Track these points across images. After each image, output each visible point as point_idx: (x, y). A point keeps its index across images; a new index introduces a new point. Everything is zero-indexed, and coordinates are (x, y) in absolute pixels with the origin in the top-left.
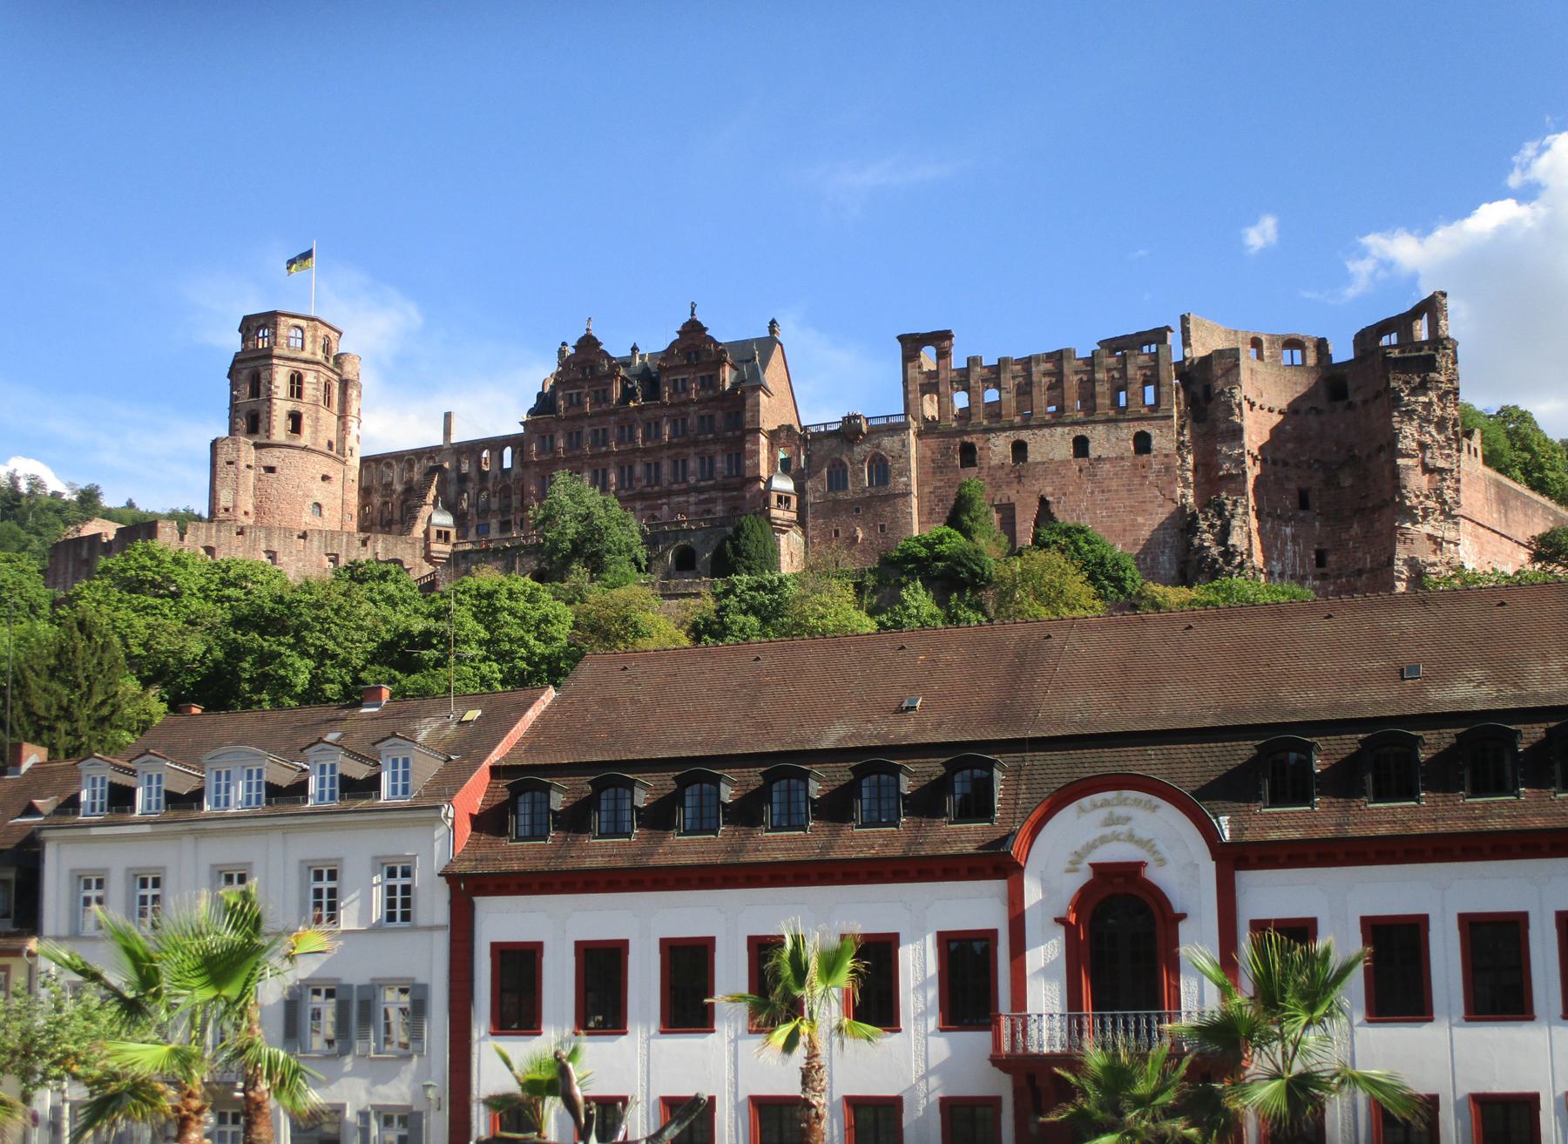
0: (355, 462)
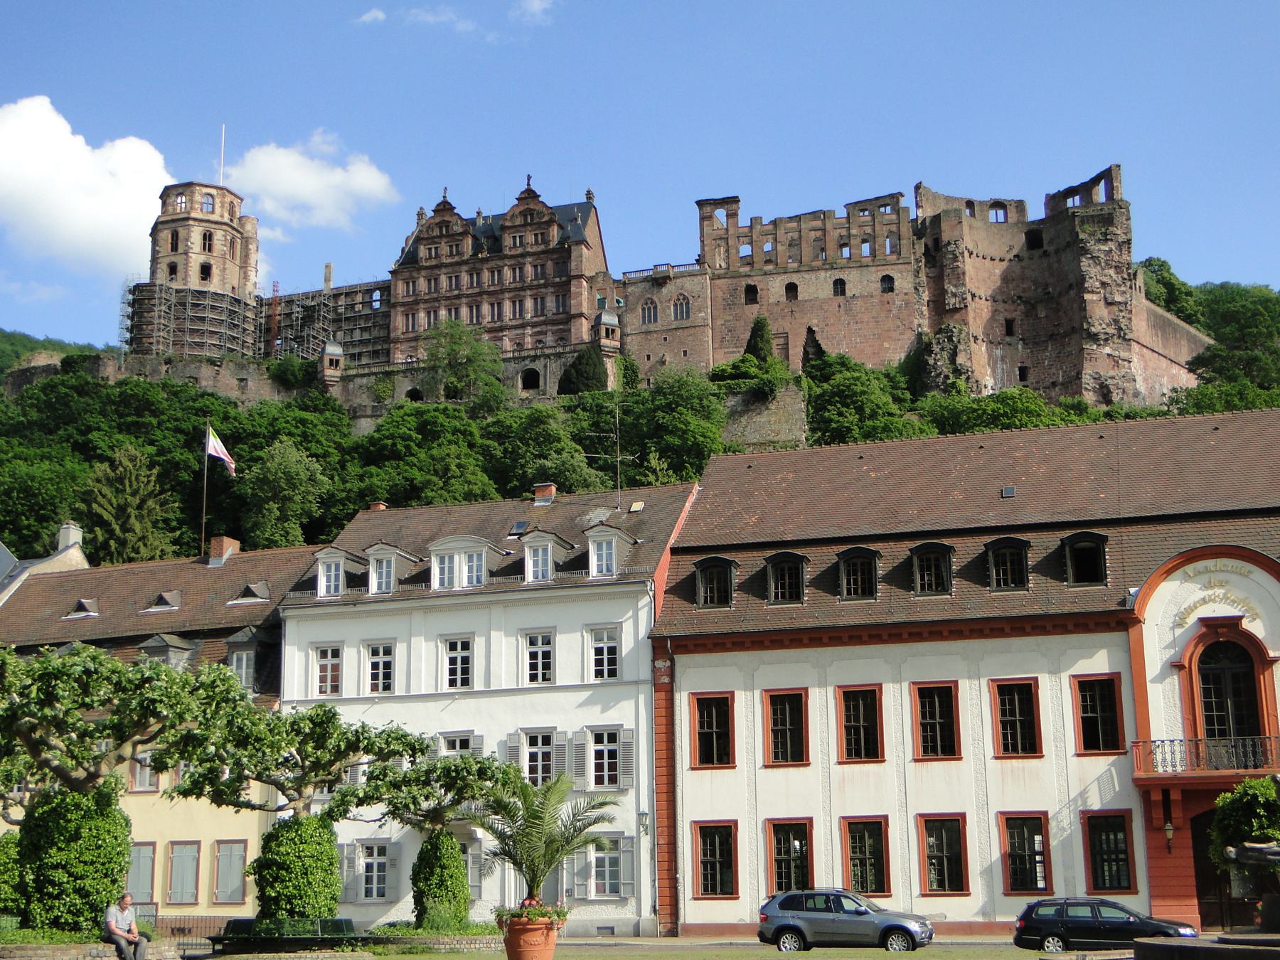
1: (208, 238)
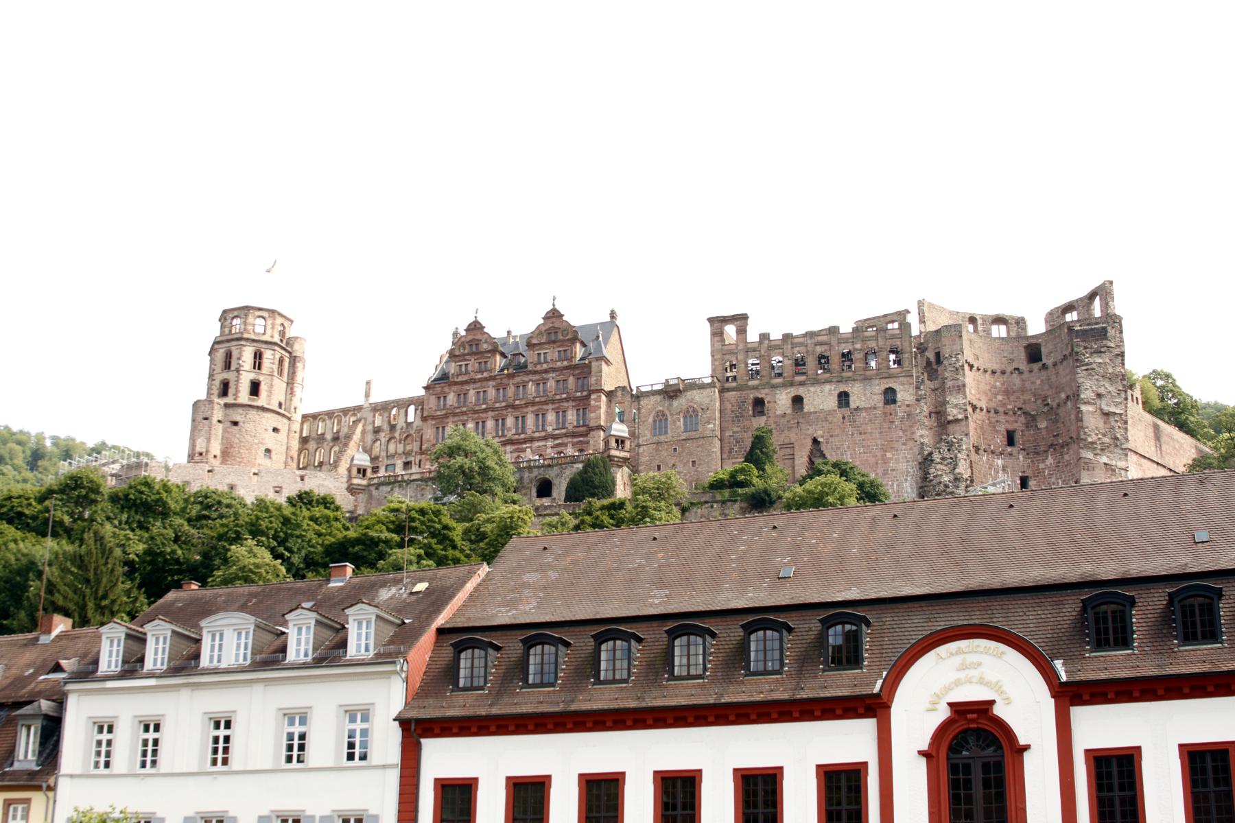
0: (297, 418)
1: (258, 356)
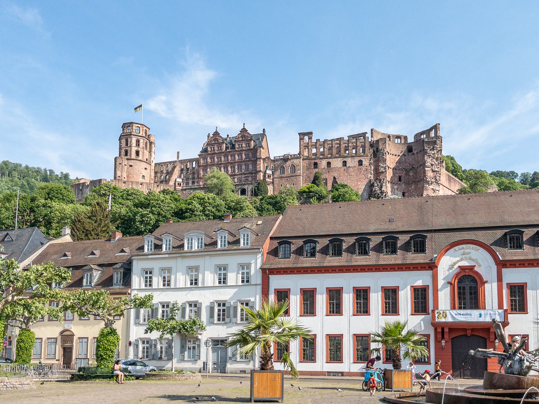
0: (153, 164)
